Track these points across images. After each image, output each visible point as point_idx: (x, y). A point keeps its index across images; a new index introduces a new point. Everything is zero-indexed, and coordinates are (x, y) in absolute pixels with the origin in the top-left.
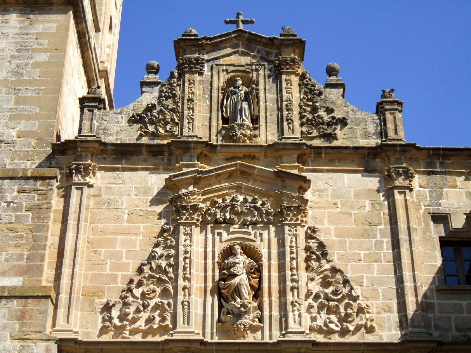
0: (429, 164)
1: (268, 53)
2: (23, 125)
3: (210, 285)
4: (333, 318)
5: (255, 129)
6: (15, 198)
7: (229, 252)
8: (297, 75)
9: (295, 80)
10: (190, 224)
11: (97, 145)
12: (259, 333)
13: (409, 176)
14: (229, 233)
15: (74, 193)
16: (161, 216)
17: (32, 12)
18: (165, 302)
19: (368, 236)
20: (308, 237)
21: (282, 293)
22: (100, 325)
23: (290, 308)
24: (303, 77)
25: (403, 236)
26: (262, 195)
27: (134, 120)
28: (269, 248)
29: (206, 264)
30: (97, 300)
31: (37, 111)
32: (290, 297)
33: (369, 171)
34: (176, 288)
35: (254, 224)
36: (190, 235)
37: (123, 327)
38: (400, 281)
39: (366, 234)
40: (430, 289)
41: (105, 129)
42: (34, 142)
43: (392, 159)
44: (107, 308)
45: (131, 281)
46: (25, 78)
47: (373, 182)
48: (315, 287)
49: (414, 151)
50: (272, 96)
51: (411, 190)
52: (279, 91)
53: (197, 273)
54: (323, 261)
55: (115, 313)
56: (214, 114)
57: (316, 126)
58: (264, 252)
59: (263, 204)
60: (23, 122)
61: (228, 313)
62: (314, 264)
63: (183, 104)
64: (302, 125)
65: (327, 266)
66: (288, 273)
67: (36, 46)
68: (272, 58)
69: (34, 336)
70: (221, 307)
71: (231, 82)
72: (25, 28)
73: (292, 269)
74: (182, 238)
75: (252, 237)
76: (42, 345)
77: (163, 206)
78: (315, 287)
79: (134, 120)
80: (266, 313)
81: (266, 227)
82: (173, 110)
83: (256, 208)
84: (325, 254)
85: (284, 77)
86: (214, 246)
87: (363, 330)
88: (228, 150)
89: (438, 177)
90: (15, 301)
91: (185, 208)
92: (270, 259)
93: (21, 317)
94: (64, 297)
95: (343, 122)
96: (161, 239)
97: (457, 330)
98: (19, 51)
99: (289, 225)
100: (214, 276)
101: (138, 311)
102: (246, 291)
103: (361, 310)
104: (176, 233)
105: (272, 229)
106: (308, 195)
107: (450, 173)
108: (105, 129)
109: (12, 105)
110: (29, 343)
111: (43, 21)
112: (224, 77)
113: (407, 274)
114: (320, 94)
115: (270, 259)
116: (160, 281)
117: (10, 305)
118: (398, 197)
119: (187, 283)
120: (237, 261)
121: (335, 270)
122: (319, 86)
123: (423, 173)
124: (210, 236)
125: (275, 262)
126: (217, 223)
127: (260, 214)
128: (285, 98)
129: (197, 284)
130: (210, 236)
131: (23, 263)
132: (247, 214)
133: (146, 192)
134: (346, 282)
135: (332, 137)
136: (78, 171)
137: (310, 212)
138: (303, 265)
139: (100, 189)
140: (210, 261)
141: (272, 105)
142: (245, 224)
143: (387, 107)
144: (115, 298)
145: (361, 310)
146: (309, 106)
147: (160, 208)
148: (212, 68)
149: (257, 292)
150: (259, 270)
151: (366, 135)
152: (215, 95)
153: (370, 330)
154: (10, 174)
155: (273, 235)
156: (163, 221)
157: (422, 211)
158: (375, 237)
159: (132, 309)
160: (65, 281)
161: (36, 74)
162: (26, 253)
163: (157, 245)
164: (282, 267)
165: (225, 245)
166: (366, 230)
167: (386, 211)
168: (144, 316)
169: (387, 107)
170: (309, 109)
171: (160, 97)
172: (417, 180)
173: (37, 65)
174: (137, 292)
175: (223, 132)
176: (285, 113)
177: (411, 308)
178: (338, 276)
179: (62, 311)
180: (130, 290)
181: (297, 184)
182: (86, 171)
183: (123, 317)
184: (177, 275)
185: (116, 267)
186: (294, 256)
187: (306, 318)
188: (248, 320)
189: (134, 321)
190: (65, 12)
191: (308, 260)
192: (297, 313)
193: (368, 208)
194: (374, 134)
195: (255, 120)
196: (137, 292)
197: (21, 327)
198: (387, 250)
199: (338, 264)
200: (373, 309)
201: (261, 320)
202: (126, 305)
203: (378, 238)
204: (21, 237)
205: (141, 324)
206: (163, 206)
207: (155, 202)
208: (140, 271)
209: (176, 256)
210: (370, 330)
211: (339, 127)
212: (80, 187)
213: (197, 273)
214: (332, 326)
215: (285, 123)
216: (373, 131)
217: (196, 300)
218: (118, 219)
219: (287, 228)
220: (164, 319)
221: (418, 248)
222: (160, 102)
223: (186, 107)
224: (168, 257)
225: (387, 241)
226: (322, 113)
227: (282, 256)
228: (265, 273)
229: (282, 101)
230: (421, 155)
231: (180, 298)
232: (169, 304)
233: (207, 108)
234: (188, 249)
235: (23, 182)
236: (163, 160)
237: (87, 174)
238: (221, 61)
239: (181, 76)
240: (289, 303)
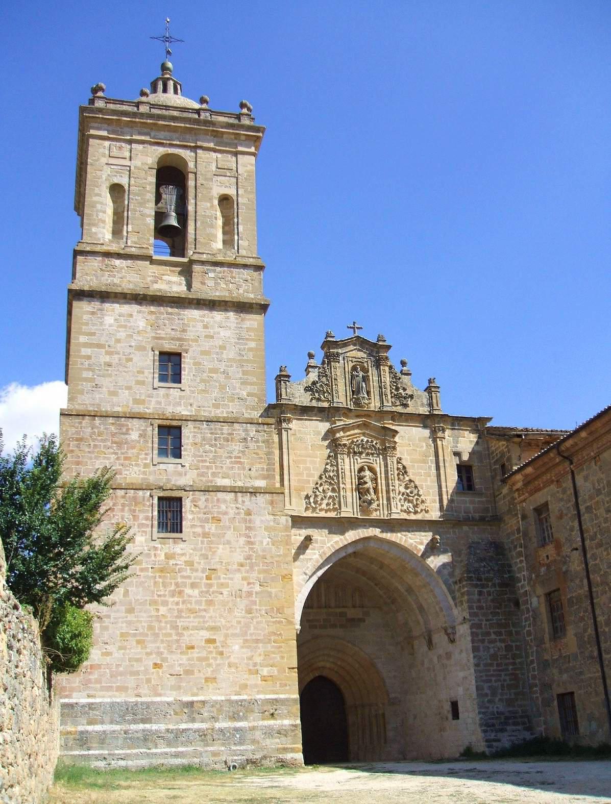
0: (453, 425)
1: (372, 351)
2: (249, 388)
3: (354, 487)
4: (410, 504)
5: (370, 399)
6: (255, 435)
7: (361, 470)
8: (387, 366)
9: (387, 369)
10: (343, 454)
11: (293, 407)
12: (378, 512)
13: (444, 431)
14: (361, 459)
15: (284, 433)
16: (327, 447)
17: (242, 312)
18: (334, 495)
19: (425, 463)
20: (398, 463)
21: (388, 492)
22: (305, 506)
23: (392, 500)
24: (391, 367)
25: (441, 464)
26: (377, 438)
27: (307, 389)
28: (380, 468)
29: (351, 475)
30: (302, 493)
31: (255, 380)
32: (392, 495)
33: (425, 427)
34: (339, 488)
35: (372, 454)
36: (343, 459)
37: (316, 508)
38: (440, 487)
39: (425, 462)
40: (453, 492)
41: (292, 394)
42: (256, 399)
43: (436, 421)
44: (307, 497)
45: (317, 484)
46: (245, 358)
47: (427, 432)
48: (402, 489)
49: (447, 418)
50: (376, 378)
51: (444, 438)
52: (380, 376)
53: (348, 480)
54: (406, 476)
55: (312, 500)
56: (348, 388)
57: (398, 398)
58: (378, 470)
59: (376, 444)
60: (249, 387)
61: (364, 502)
62: (401, 477)
63: (332, 381)
64: (392, 397)
65: (407, 478)
66: (390, 482)
67: (247, 337)
68: (374, 354)
69: (279, 513)
70: (360, 498)
71: (354, 368)
72: (240, 323)
73: (392, 480)
74: (340, 461)
75: (371, 461)
76: (284, 518)
77: (328, 442)
78: (402, 489)
79: (307, 389)
80: (381, 502)
81: (378, 455)
82: (326, 384)
83: (373, 446)
84: (406, 472)
85: (382, 367)
86: (354, 466)
87: (424, 511)
88: (357, 411)
89: (456, 431)
90: (267, 495)
91: (340, 445)
92: (381, 474)
93: (272, 503)
94: (287, 491)
95: (411, 397)
96: (329, 461)
97: (465, 513)
98: (239, 339)
99: (389, 456)
100: (355, 482)
101: (322, 499)
102: (372, 491)
103: (423, 502)
104: (336, 458)
105: (381, 457)
106: (397, 439)
107: (462, 430)
108: (292, 394)
109: (240, 375)
110: (277, 517)
111: (249, 319)
112: (351, 365)
113: (443, 484)
114: (400, 378)
115: (381, 474)
116: (330, 484)
117: (265, 497)
118: (439, 443)
119: (344, 486)
120: (365, 474)
121: (410, 481)
122: (399, 374)
123: (450, 429)
124: (352, 460)
125: (383, 475)
126: (355, 453)
127: (375, 448)
128: (383, 381)
129: (349, 486)
130: (352, 460)
131: (265, 473)
132: (369, 449)
133: (319, 433)
134: (416, 487)
135: (405, 406)
136: (285, 421)
137: (398, 449)
138: (396, 477)
139: (295, 430)
140: (353, 474)
141: (376, 384)
142: (368, 454)
143: (433, 389)
144: (310, 493)
145: (423, 502)
146: (394, 385)
147: (326, 443)
148: (344, 358)
149: (376, 490)
150: (376, 479)
151: (422, 405)
152: (347, 376)
153: (427, 512)
154: (250, 421)
155: (381, 460)
156: (329, 450)
157: (449, 450)
158: (428, 463)
159: (320, 498)
160: (286, 483)
161: (250, 356)
162: (265, 467)
163: (327, 464)
164: (387, 478)
165: (360, 465)
166: (424, 460)
167: (433, 449)
168: (325, 502)
169: (433, 389)
170: (394, 387)
171: (319, 376)
172: (448, 432)
173: (250, 349)
174: (321, 489)
175: (354, 400)
176: (384, 390)
177: (445, 502)
178: (412, 484)
179: (287, 499)
180: (317, 488)
181: (392, 434)
182: (289, 421)
183: (316, 502)
184: (339, 481)
185: (309, 475)
186: (392, 473)
187: (399, 507)
188: (374, 506)
189: (321, 504)
190: (261, 314)
191: (398, 474)
192: (395, 503)
193: (425, 448)
194: (427, 405)
195: (368, 393)
196: (321, 489)
197: (272, 509)
198: (434, 471)
199: (412, 477)
200: (428, 501)
201: (378, 505)
202: (316, 496)
203: (430, 464)
204: (261, 458)
205: (324, 506)
206: (328, 442)
207: (324, 439)
208: (321, 478)
209: (338, 469)
210: (427, 512)
211: (409, 399)
212: (287, 430)
213: (348, 480)
214: (410, 509)
215: (384, 396)
216: (426, 403)
217: (349, 494)
218: (306, 448)
219: (388, 458)
220: (334, 504)
221: (448, 470)
222: (319, 379)
223: (333, 383)
224: (333, 471)
225: (434, 466)
226: (401, 391)
227: (386, 472)
228: (379, 481)
229: (381, 383)
230: (450, 419)
231: (342, 493)
232: (336, 496)
233: (344, 384)
234: (343, 467)
235: (257, 426)
236: (325, 415)
237: (289, 423)
238: (348, 354)
239: (329, 363)
240: (391, 498)
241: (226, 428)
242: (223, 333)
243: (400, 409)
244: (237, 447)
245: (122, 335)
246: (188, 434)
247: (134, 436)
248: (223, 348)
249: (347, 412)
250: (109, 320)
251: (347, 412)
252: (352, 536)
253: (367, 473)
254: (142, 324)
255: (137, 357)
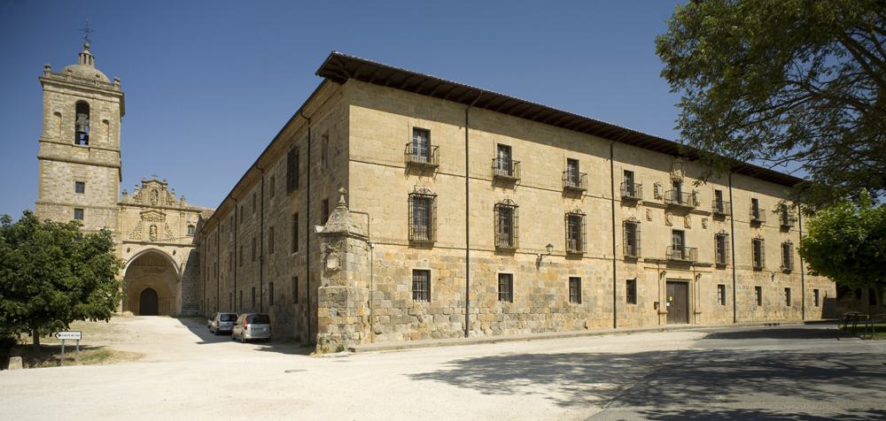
241: (101, 211)
242: (102, 176)
243: (168, 206)
244: (105, 217)
245: (60, 175)
246: (86, 212)
247: (65, 212)
248: (101, 181)
249: (148, 207)
250: (55, 169)
251: (148, 207)
252: (145, 248)
253: (154, 228)
254: (68, 171)
255: (66, 183)
